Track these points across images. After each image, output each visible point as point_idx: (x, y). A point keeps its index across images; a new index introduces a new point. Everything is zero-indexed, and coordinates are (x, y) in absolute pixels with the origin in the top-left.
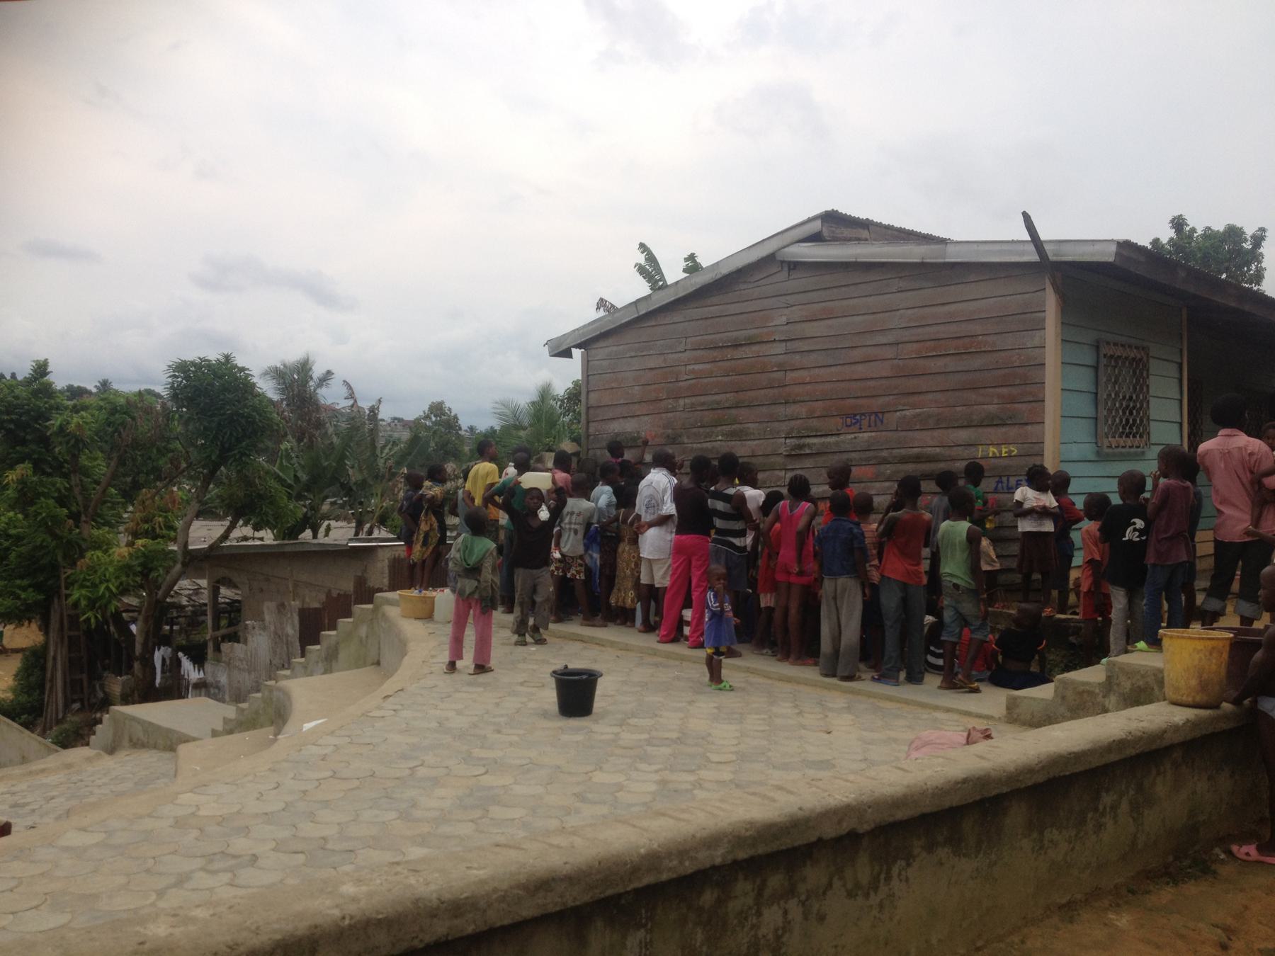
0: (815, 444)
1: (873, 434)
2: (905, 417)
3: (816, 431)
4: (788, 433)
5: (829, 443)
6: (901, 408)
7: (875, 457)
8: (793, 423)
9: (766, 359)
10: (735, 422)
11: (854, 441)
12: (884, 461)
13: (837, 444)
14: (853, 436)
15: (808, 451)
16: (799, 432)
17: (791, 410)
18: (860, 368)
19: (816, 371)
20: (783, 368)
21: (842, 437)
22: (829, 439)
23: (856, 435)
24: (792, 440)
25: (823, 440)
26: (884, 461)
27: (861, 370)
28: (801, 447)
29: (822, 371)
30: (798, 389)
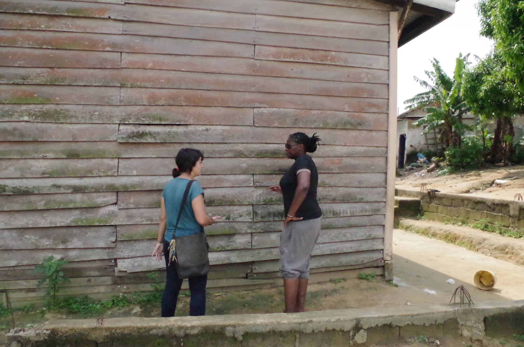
0: (158, 134)
1: (227, 128)
2: (262, 114)
3: (160, 119)
4: (124, 119)
5: (176, 133)
6: (257, 105)
7: (231, 151)
8: (129, 109)
9: (95, 37)
10: (48, 100)
11: (205, 132)
12: (239, 155)
13: (186, 134)
14: (204, 128)
15: (150, 140)
16: (138, 119)
17: (125, 93)
18: (213, 62)
19: (161, 58)
20: (116, 48)
21: (190, 128)
22: (175, 129)
23: (208, 127)
24: (128, 127)
25: (167, 129)
26: (239, 155)
27: (214, 63)
28: (142, 135)
29: (167, 59)
30: (135, 74)
